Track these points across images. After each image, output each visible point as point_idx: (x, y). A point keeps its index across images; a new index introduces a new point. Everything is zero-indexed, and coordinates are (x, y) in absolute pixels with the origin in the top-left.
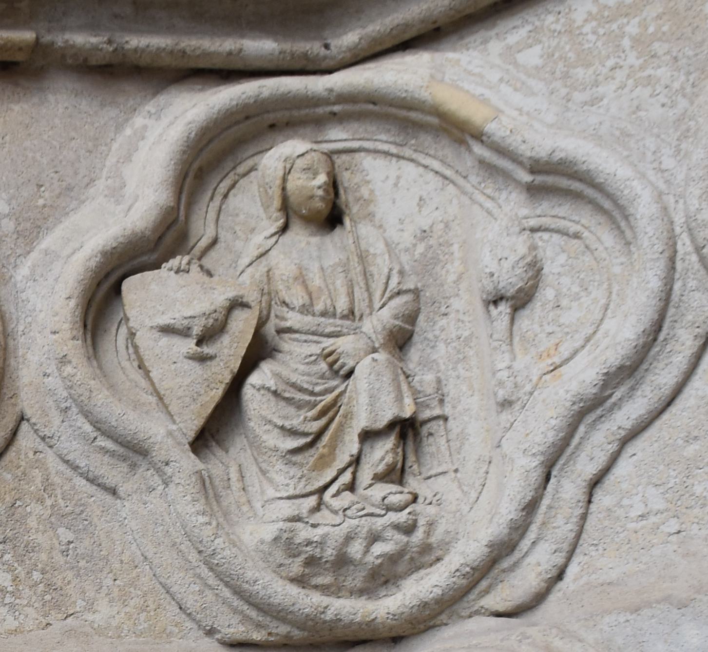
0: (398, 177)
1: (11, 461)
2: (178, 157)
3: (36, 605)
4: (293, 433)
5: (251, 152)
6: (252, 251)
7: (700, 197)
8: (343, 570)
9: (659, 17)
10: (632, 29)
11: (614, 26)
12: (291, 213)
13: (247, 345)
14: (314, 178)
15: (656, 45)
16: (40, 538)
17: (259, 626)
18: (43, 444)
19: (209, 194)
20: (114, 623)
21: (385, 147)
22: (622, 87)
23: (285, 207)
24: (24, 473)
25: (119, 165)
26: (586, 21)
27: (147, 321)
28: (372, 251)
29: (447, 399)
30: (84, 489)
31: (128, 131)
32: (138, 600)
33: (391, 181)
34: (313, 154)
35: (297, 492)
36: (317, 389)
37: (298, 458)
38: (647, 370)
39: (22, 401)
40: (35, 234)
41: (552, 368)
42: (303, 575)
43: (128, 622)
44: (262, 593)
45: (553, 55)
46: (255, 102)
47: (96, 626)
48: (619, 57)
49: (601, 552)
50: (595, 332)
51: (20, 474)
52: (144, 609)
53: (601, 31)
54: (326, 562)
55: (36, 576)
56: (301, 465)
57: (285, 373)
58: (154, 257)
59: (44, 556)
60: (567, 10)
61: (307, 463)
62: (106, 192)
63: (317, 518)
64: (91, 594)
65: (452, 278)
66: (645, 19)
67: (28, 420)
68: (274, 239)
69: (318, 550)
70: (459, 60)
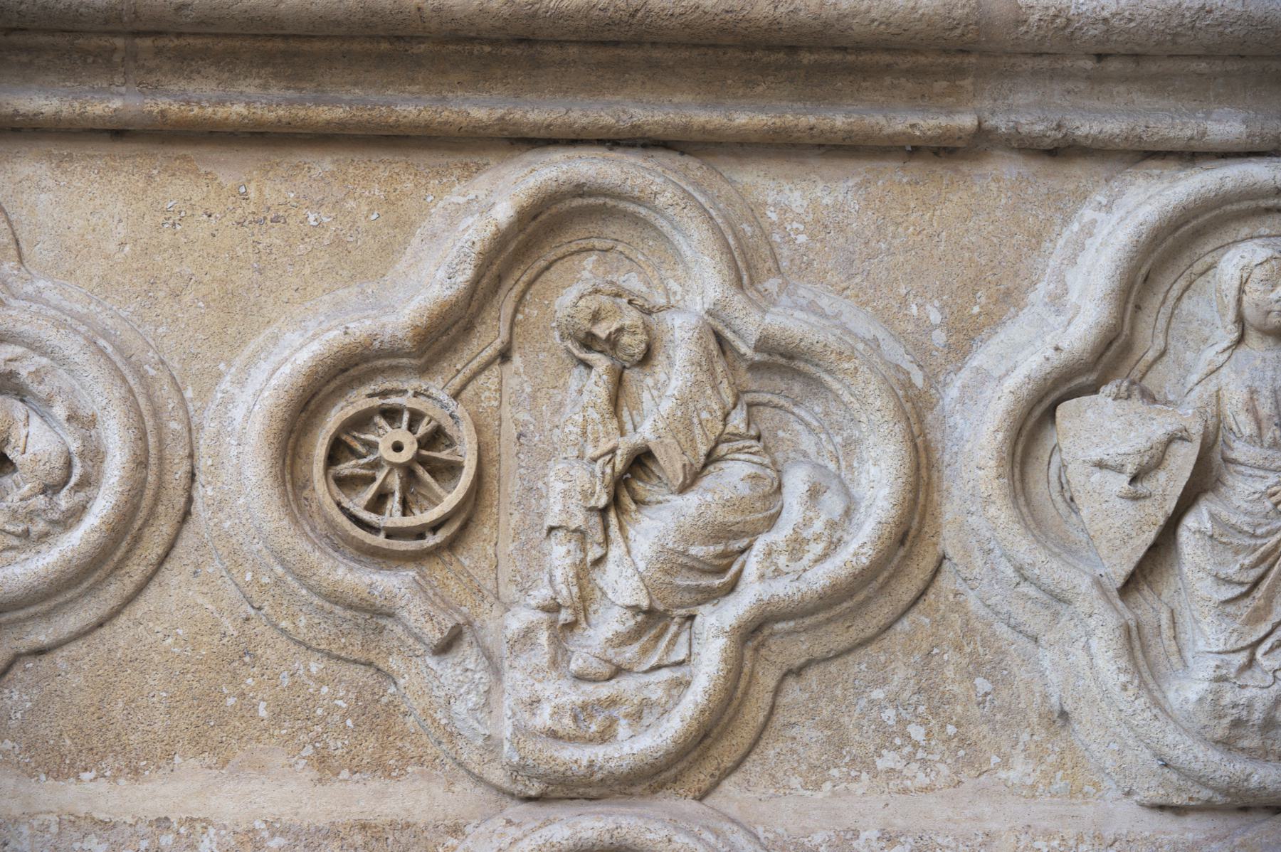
1: (930, 605)
2: (1125, 265)
3: (949, 761)
4: (1228, 581)
5: (1209, 248)
6: (1201, 369)
8: (1272, 734)
12: (1247, 325)
13: (1184, 483)
14: (1272, 291)
16: (956, 688)
17: (1179, 790)
18: (964, 585)
19: (1161, 297)
20: (1029, 781)
23: (1240, 320)
24: (943, 617)
25: (1063, 267)
27: (1080, 453)
30: (1005, 635)
31: (1075, 227)
32: (1055, 757)
34: (1273, 262)
35: (1228, 647)
36: (1259, 532)
37: (1231, 609)
39: (944, 540)
40: (968, 346)
42: (1228, 738)
43: (1043, 781)
44: (1182, 758)
46: (1216, 195)
47: (1010, 784)
51: (938, 618)
52: (1061, 765)
54: (1253, 725)
55: (951, 729)
56: (1235, 617)
57: (1224, 514)
58: (1092, 377)
59: (959, 709)
61: (1242, 615)
62: (1046, 300)
63: (1246, 678)
64: (1005, 749)
67: (950, 560)
68: (1226, 355)
69: (1245, 713)
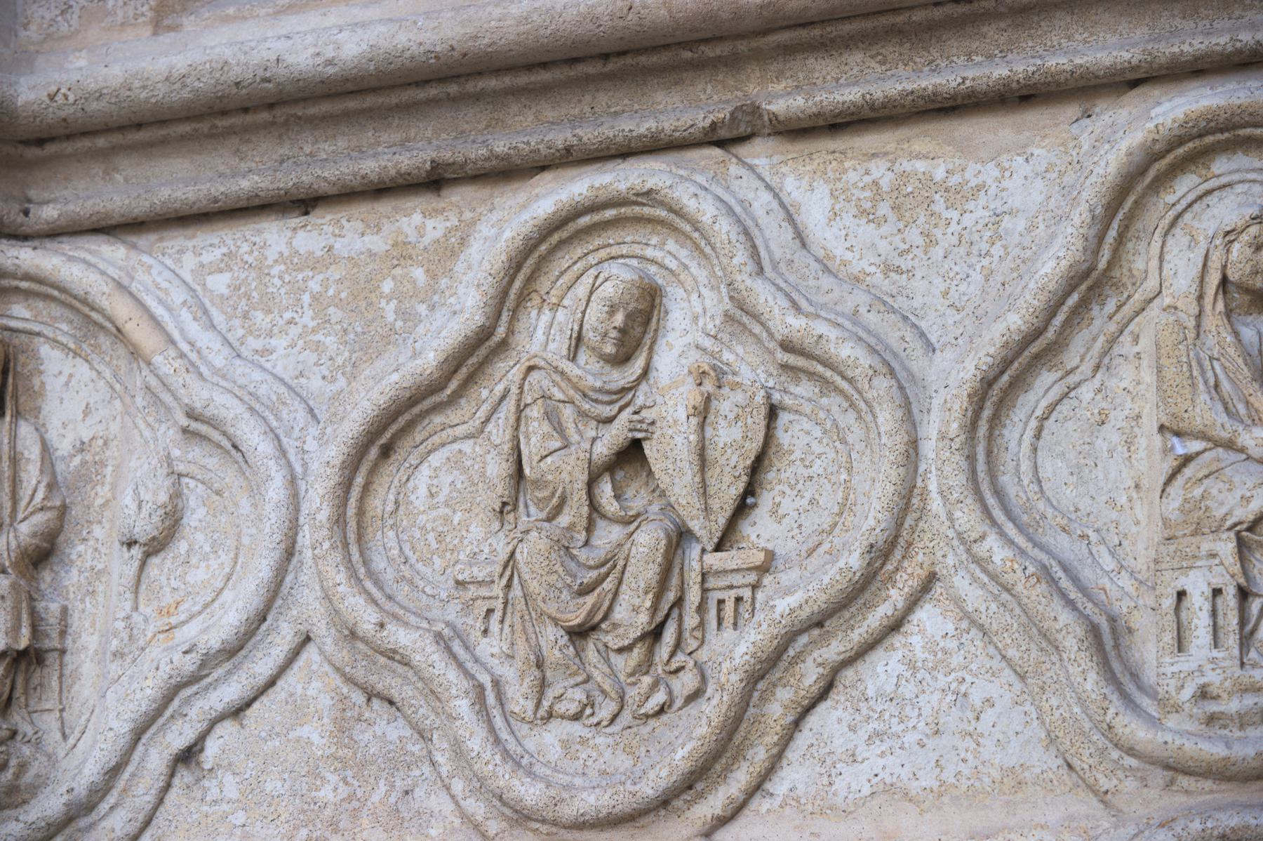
0: (71, 376)
7: (323, 496)
9: (340, 281)
10: (314, 285)
11: (300, 277)
15: (332, 310)
21: (64, 339)
22: (293, 346)
26: (276, 261)
28: (26, 453)
29: (70, 631)
33: (63, 379)
38: (245, 657)
41: (167, 628)
45: (239, 289)
48: (297, 312)
49: (173, 828)
50: (213, 601)
53: (287, 278)
60: (262, 244)
65: (99, 501)
66: (328, 279)
70: (150, 267)
